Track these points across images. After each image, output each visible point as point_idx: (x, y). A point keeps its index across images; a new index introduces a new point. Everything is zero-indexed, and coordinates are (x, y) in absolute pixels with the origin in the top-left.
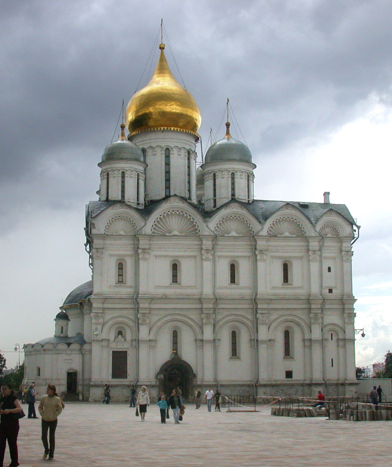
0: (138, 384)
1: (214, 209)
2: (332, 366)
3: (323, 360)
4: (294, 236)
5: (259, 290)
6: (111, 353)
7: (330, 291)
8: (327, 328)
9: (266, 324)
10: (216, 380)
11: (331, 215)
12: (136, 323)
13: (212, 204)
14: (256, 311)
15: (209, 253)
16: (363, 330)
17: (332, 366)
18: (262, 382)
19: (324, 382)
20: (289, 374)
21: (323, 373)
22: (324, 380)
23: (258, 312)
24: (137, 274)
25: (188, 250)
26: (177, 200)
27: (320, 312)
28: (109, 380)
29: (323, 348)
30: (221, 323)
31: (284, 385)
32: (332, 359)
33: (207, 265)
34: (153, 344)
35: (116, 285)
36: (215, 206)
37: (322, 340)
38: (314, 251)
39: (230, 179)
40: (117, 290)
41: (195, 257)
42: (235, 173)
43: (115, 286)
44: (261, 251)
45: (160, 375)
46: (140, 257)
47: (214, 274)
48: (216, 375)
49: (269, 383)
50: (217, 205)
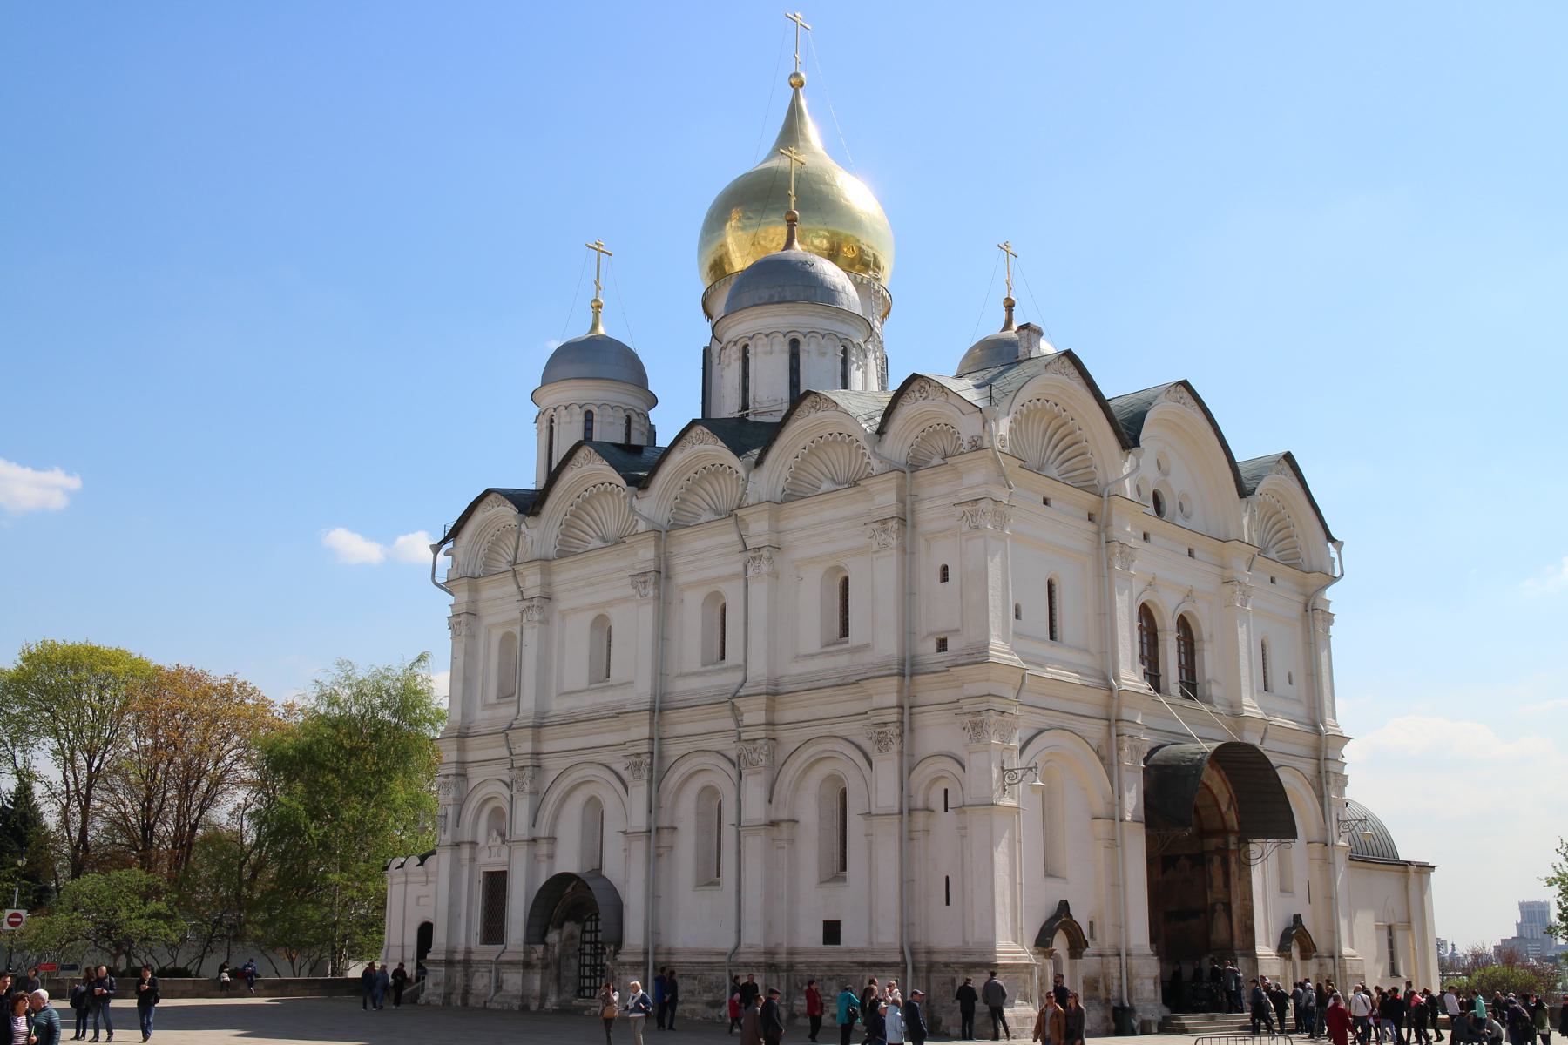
0: (504, 958)
2: (948, 903)
3: (906, 883)
4: (846, 486)
7: (942, 645)
8: (923, 774)
9: (760, 773)
10: (646, 953)
11: (924, 396)
14: (740, 734)
16: (1036, 768)
17: (948, 903)
18: (743, 959)
19: (898, 958)
20: (832, 931)
21: (906, 924)
22: (902, 952)
23: (744, 736)
27: (895, 718)
28: (473, 948)
29: (907, 839)
30: (673, 779)
31: (810, 965)
32: (947, 878)
33: (647, 613)
34: (543, 848)
37: (901, 813)
38: (884, 521)
45: (552, 931)
47: (662, 637)
48: (653, 929)
49: (762, 959)
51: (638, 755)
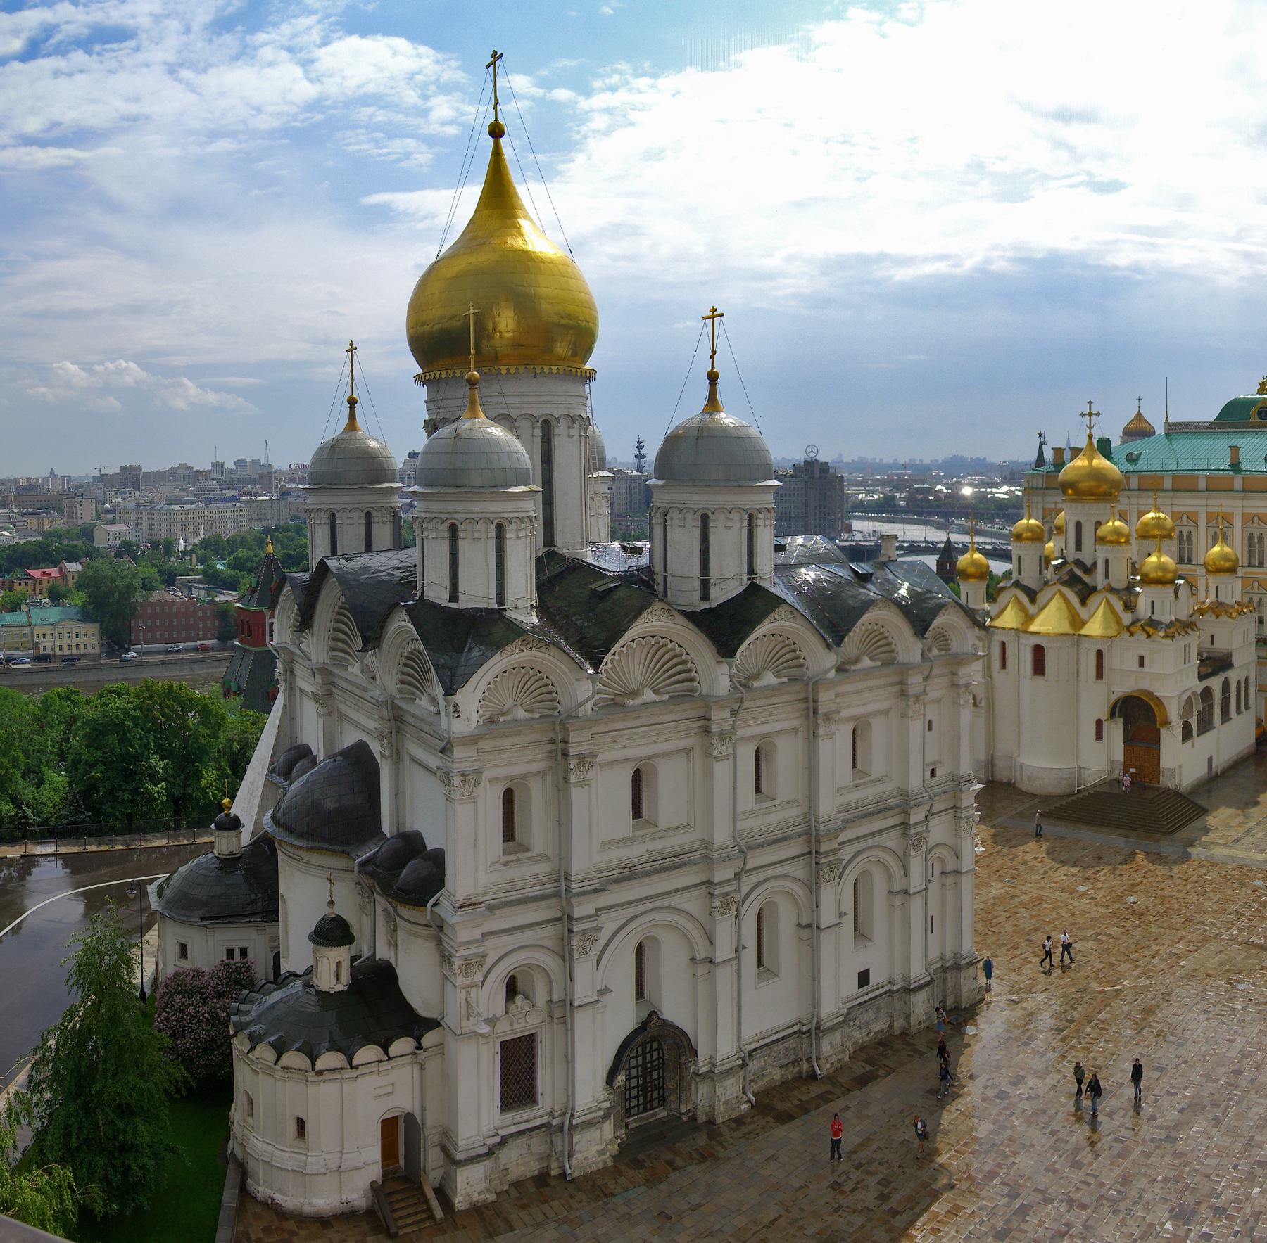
1: (705, 606)
5: (821, 808)
6: (498, 1049)
12: (563, 958)
13: (698, 594)
15: (725, 739)
20: (864, 978)
24: (562, 823)
25: (677, 736)
26: (658, 613)
35: (506, 859)
36: (705, 596)
39: (745, 531)
40: (510, 873)
41: (689, 751)
42: (756, 514)
43: (505, 864)
44: (827, 717)
46: (573, 778)
50: (712, 596)
51: (726, 894)
